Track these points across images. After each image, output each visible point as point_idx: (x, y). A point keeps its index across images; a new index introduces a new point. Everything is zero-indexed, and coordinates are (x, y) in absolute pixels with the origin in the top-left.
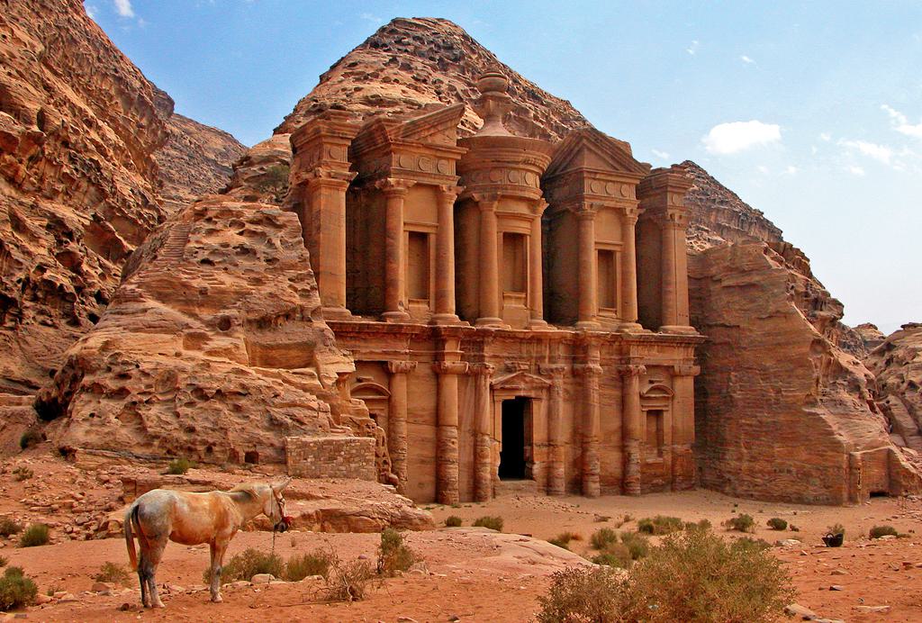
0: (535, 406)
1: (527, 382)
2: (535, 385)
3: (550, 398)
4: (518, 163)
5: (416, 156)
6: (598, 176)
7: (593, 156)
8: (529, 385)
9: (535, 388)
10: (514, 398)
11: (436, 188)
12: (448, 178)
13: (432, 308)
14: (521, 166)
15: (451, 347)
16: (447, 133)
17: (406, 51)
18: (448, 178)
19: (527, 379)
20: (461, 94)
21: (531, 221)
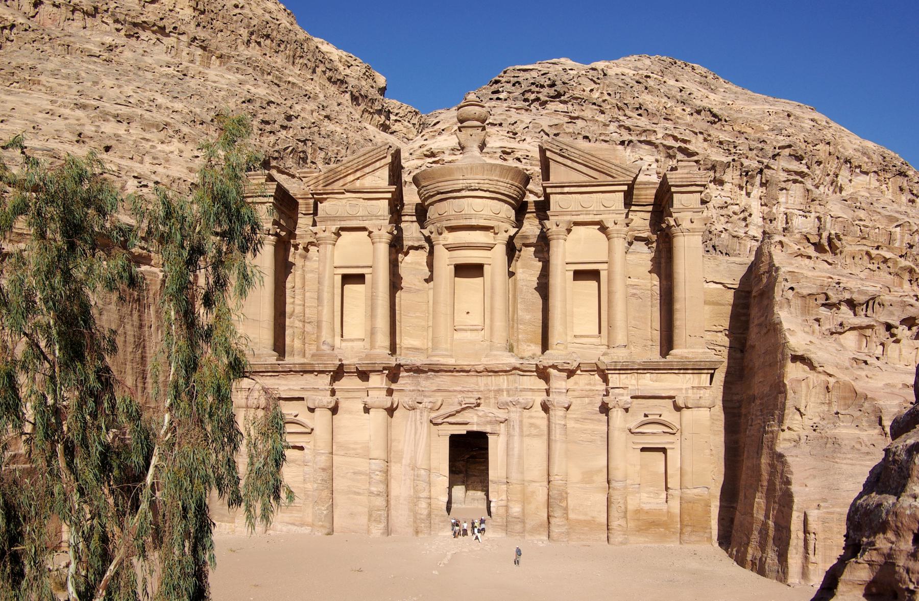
0: (491, 439)
1: (479, 416)
2: (489, 419)
3: (509, 435)
4: (459, 191)
5: (344, 201)
6: (566, 190)
7: (563, 168)
8: (483, 419)
9: (490, 423)
10: (465, 432)
11: (364, 229)
12: (377, 217)
13: (368, 346)
14: (464, 193)
15: (377, 381)
16: (377, 173)
17: (498, 99)
18: (377, 217)
19: (480, 414)
20: (547, 130)
21: (490, 248)
